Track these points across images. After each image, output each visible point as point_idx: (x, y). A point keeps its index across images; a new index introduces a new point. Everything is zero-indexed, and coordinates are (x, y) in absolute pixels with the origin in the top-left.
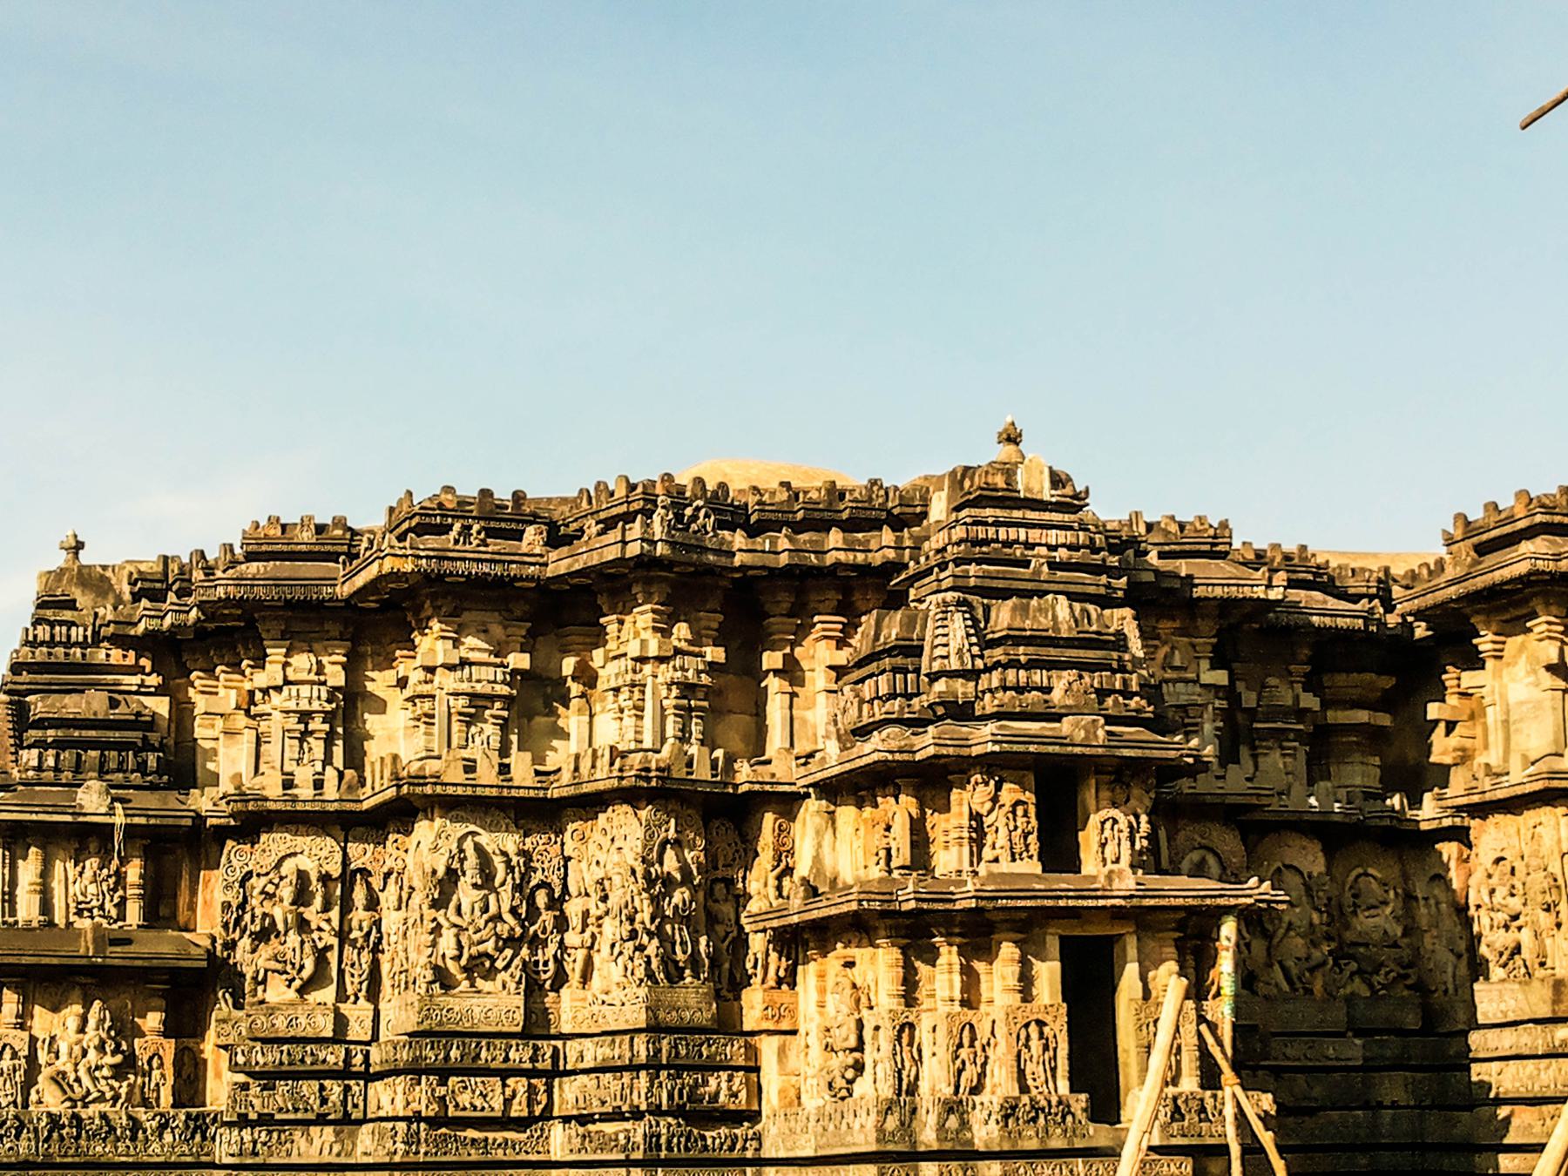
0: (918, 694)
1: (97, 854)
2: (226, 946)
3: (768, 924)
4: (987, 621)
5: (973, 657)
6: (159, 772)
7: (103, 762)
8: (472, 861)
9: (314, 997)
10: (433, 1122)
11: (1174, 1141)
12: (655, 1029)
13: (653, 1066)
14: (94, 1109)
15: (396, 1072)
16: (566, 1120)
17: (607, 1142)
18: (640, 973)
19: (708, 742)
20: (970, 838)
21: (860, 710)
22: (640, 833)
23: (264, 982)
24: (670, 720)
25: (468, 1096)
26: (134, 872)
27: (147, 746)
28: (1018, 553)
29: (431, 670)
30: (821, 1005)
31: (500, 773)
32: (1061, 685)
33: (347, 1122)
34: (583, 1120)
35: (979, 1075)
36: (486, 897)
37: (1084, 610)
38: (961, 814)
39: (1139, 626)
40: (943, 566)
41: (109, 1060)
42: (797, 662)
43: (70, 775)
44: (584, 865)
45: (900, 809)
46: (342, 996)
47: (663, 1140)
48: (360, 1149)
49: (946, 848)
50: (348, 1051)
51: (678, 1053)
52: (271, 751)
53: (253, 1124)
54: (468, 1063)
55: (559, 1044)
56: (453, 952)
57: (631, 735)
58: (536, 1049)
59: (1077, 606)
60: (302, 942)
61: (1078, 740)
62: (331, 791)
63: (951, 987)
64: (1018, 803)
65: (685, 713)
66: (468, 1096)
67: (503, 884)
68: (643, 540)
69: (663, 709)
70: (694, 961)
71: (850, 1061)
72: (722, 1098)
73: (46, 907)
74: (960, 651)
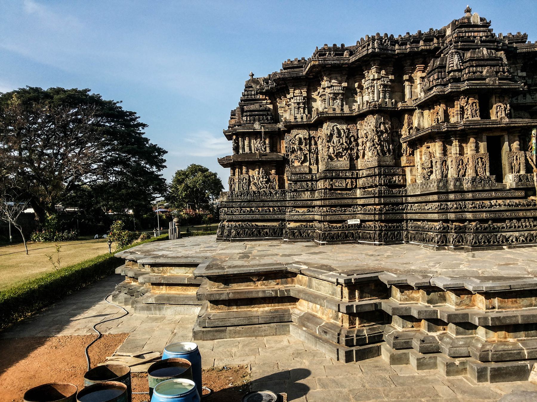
0: (445, 78)
1: (260, 138)
2: (287, 155)
3: (407, 140)
4: (464, 56)
5: (460, 66)
6: (271, 120)
7: (259, 118)
8: (336, 131)
9: (305, 164)
10: (330, 190)
11: (520, 187)
12: (380, 166)
13: (380, 175)
14: (262, 189)
15: (321, 179)
16: (360, 188)
17: (369, 193)
18: (376, 154)
19: (391, 98)
20: (460, 113)
21: (430, 84)
22: (375, 121)
23: (294, 162)
24: (381, 93)
25: (337, 184)
26: (267, 141)
27: (268, 115)
28: (472, 39)
29: (324, 89)
30: (421, 159)
31: (341, 110)
32: (485, 71)
33: (313, 191)
34: (364, 188)
35: (464, 172)
36: (339, 139)
37: (490, 51)
38: (457, 107)
39: (506, 56)
40: (451, 44)
41: (264, 180)
42: (412, 78)
43: (252, 121)
44: (362, 131)
45: (440, 108)
46: (310, 164)
47: (383, 192)
48: (316, 196)
49: (453, 117)
50: (312, 176)
51: (385, 172)
52: (293, 112)
53: (293, 192)
54: (337, 176)
55: (358, 171)
56: (332, 152)
57: (372, 99)
58: (352, 173)
59: (489, 51)
60: (301, 153)
61: (491, 84)
62: (305, 120)
63: (456, 150)
64: (473, 104)
65: (385, 92)
66: (337, 184)
67: (343, 136)
68: (372, 48)
69: (379, 91)
70: (389, 150)
71: (429, 170)
72: (397, 182)
73: (250, 149)
74: (457, 65)
